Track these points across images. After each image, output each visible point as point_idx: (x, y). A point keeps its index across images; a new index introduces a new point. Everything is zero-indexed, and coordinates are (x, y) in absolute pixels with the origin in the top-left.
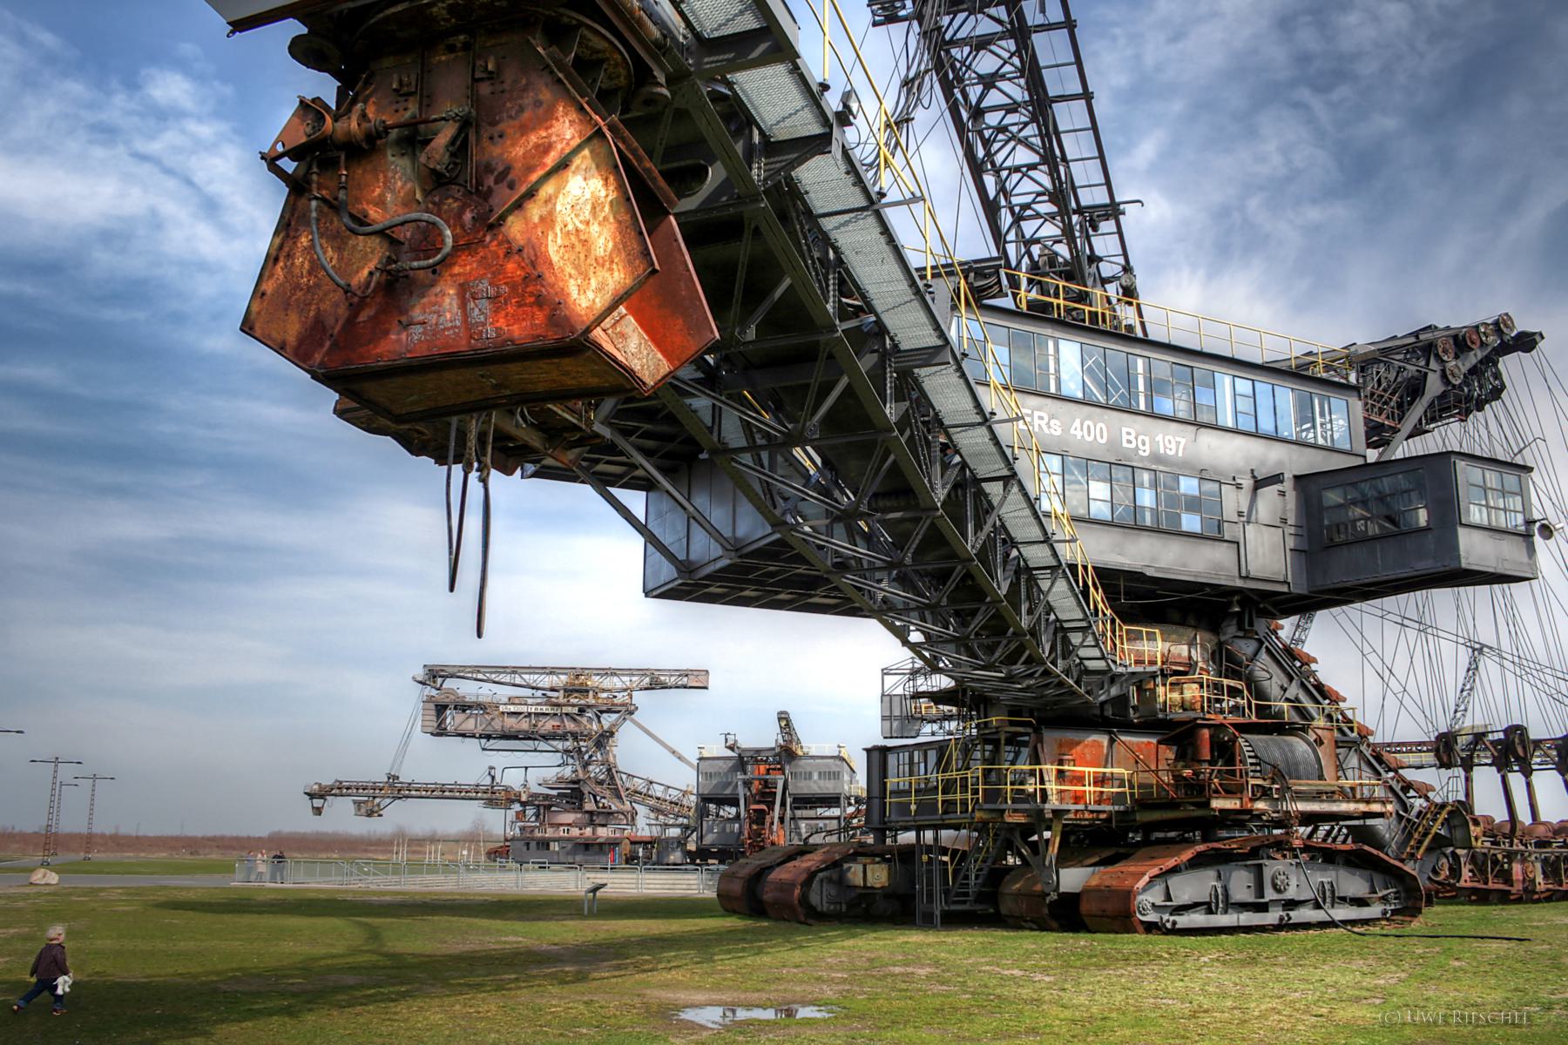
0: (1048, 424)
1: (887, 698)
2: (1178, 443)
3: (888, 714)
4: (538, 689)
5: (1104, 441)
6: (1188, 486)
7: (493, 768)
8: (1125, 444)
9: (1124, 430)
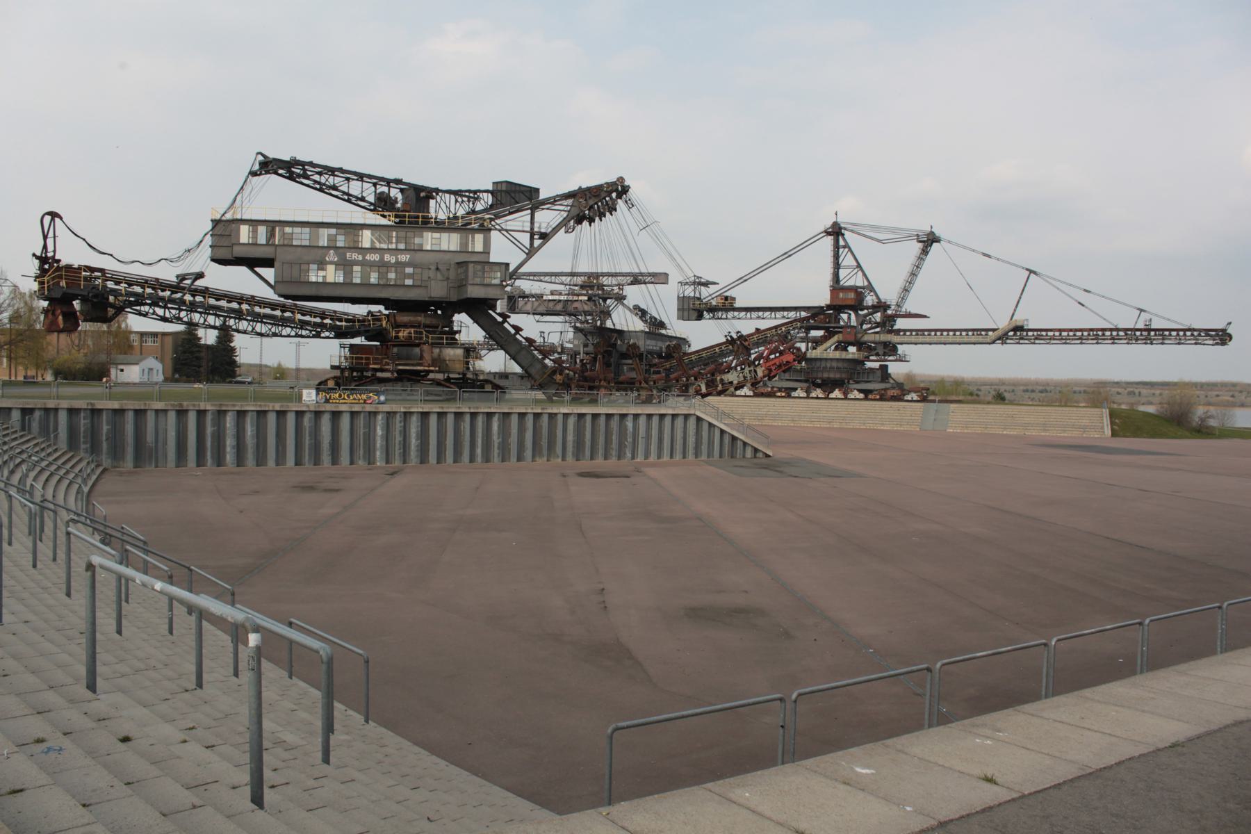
2: (406, 257)
4: (566, 285)
6: (409, 270)
7: (543, 333)
9: (386, 255)
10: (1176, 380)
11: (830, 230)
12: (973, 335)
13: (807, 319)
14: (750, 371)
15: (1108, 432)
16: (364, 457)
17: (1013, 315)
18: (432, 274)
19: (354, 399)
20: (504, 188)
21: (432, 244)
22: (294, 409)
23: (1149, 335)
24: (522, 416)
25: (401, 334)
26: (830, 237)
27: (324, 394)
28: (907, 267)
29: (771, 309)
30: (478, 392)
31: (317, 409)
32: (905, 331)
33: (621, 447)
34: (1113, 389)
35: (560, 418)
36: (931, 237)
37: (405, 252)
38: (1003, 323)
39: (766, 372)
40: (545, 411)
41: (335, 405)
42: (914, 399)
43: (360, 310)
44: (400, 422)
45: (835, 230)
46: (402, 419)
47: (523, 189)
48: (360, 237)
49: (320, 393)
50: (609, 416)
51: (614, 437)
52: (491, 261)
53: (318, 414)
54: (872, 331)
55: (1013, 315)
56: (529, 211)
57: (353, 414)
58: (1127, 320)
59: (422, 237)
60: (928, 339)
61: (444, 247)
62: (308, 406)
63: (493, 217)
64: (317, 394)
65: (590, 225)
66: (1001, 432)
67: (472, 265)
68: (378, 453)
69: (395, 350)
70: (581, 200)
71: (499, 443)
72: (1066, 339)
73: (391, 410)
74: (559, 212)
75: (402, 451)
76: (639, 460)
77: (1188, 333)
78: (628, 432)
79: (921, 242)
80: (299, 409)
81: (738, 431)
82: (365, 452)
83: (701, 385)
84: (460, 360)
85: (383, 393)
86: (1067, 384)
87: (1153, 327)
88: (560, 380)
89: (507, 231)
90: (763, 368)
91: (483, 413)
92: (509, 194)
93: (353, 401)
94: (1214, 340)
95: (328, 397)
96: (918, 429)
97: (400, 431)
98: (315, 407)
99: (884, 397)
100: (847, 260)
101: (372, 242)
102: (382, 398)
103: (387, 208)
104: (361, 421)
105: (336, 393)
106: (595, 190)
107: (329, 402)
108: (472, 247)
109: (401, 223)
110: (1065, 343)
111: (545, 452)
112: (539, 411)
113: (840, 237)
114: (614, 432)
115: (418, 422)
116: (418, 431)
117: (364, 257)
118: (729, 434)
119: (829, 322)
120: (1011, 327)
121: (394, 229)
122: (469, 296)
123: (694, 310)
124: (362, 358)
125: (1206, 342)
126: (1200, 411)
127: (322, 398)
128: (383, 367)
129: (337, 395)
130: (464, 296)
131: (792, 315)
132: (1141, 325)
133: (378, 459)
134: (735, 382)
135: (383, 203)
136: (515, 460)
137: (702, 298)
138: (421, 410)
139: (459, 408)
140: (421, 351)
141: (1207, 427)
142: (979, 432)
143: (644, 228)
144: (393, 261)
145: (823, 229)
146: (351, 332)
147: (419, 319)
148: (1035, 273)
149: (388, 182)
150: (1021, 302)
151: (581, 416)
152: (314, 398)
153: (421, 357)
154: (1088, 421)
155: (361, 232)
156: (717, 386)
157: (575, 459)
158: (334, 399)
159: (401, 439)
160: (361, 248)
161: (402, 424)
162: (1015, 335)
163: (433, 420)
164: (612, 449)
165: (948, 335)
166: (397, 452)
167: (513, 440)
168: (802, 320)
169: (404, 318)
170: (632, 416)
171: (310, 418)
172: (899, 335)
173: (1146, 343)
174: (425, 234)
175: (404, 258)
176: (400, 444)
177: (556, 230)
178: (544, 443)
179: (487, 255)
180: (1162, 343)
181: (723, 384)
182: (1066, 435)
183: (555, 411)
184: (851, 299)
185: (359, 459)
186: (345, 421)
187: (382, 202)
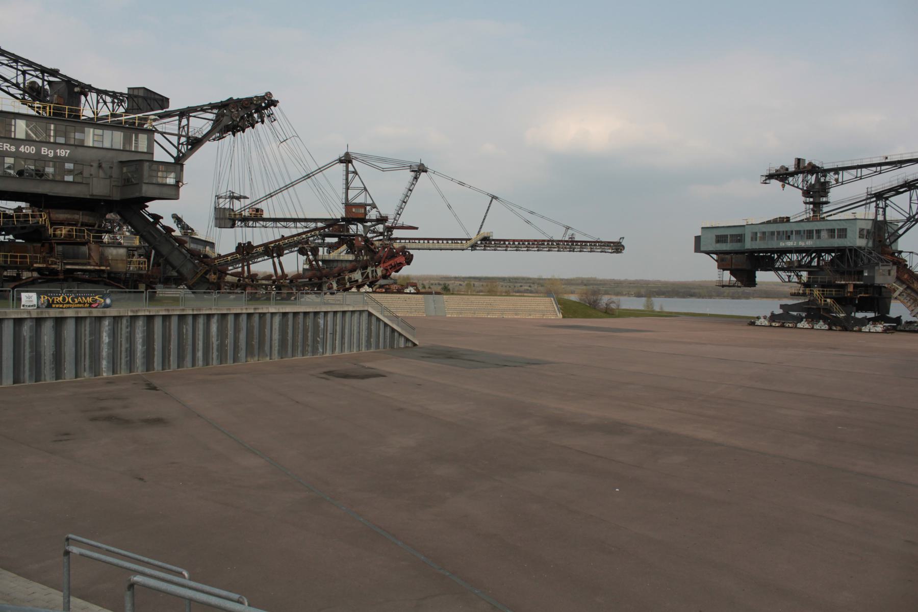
0: (10, 148)
1: (217, 210)
2: (66, 152)
3: (218, 217)
5: (34, 152)
6: (69, 166)
8: (43, 153)
9: (43, 148)
10: (549, 277)
11: (343, 158)
12: (410, 242)
13: (323, 228)
14: (373, 271)
15: (560, 316)
16: (91, 368)
17: (481, 228)
18: (93, 171)
19: (79, 303)
20: (141, 93)
21: (94, 141)
22: (13, 317)
23: (571, 245)
24: (237, 316)
25: (58, 232)
26: (342, 164)
27: (46, 297)
28: (403, 190)
29: (295, 220)
30: (130, 292)
31: (40, 316)
32: (401, 239)
33: (315, 341)
34: (456, 282)
35: (268, 316)
36: (421, 168)
37: (65, 146)
38: (473, 235)
39: (384, 272)
40: (257, 311)
41: (61, 310)
42: (412, 292)
43: (13, 205)
44: (127, 328)
45: (348, 159)
46: (129, 324)
47: (156, 97)
48: (13, 127)
49: (42, 296)
50: (306, 314)
51: (309, 334)
52: (155, 159)
53: (39, 321)
54: (377, 238)
55: (481, 228)
56: (177, 118)
57: (78, 320)
58: (558, 235)
59: (83, 132)
60: (431, 245)
61: (107, 145)
62: (29, 312)
63: (157, 117)
64: (39, 298)
65: (234, 136)
66: (486, 316)
67: (148, 163)
68: (104, 363)
69: (59, 248)
70: (233, 110)
71: (218, 345)
72: (518, 247)
73: (119, 315)
74: (207, 121)
75: (129, 358)
76: (327, 355)
77: (597, 244)
78: (320, 329)
79: (412, 171)
80: (19, 316)
81: (398, 325)
82: (91, 362)
83: (333, 283)
84: (122, 260)
85: (108, 295)
86: (604, 280)
87: (576, 239)
88: (214, 279)
89: (162, 133)
90: (382, 269)
91: (203, 314)
92: (146, 101)
93: (78, 305)
94: (612, 249)
95: (51, 300)
96: (425, 315)
97: (127, 337)
98: (38, 313)
99: (389, 290)
100: (356, 183)
101: (27, 133)
102: (108, 301)
103: (41, 99)
104: (87, 327)
105: (59, 297)
106: (246, 102)
107: (52, 307)
108: (135, 146)
109: (57, 115)
110: (517, 250)
111: (256, 351)
112: (252, 311)
113: (350, 165)
114: (310, 329)
115: (144, 327)
116: (144, 336)
117: (17, 149)
118: (390, 326)
119: (342, 232)
120: (480, 237)
121: (51, 121)
122: (144, 195)
123: (230, 219)
124: (16, 257)
125: (606, 250)
126: (605, 299)
127: (44, 302)
128: (49, 266)
129: (61, 299)
130: (141, 195)
131: (312, 225)
132: (567, 239)
133: (104, 369)
134: (360, 280)
135: (33, 93)
136: (232, 361)
137: (235, 210)
138: (147, 313)
139: (183, 310)
140: (89, 249)
141: (612, 310)
142: (470, 316)
143: (284, 141)
144: (51, 155)
145: (337, 157)
146: (7, 228)
147: (76, 217)
148: (496, 198)
149: (44, 70)
150: (487, 217)
151: (285, 314)
152: (35, 302)
153: (90, 257)
154: (544, 307)
155: (13, 121)
156: (345, 284)
157: (280, 358)
158: (58, 303)
159: (128, 345)
160: (15, 139)
161: (129, 330)
162: (481, 243)
163: (158, 324)
164: (308, 346)
165: (443, 243)
166: (123, 361)
167: (230, 341)
168: (316, 229)
169: (61, 215)
170: (323, 314)
171: (31, 327)
172: (396, 242)
173: (570, 251)
174: (86, 129)
175: (63, 153)
176: (126, 351)
177: (207, 137)
178: (255, 342)
179: (151, 155)
180: (580, 251)
181: (350, 283)
182: (532, 317)
183: (265, 311)
184: (362, 213)
185: (85, 371)
186: (69, 330)
187: (34, 92)
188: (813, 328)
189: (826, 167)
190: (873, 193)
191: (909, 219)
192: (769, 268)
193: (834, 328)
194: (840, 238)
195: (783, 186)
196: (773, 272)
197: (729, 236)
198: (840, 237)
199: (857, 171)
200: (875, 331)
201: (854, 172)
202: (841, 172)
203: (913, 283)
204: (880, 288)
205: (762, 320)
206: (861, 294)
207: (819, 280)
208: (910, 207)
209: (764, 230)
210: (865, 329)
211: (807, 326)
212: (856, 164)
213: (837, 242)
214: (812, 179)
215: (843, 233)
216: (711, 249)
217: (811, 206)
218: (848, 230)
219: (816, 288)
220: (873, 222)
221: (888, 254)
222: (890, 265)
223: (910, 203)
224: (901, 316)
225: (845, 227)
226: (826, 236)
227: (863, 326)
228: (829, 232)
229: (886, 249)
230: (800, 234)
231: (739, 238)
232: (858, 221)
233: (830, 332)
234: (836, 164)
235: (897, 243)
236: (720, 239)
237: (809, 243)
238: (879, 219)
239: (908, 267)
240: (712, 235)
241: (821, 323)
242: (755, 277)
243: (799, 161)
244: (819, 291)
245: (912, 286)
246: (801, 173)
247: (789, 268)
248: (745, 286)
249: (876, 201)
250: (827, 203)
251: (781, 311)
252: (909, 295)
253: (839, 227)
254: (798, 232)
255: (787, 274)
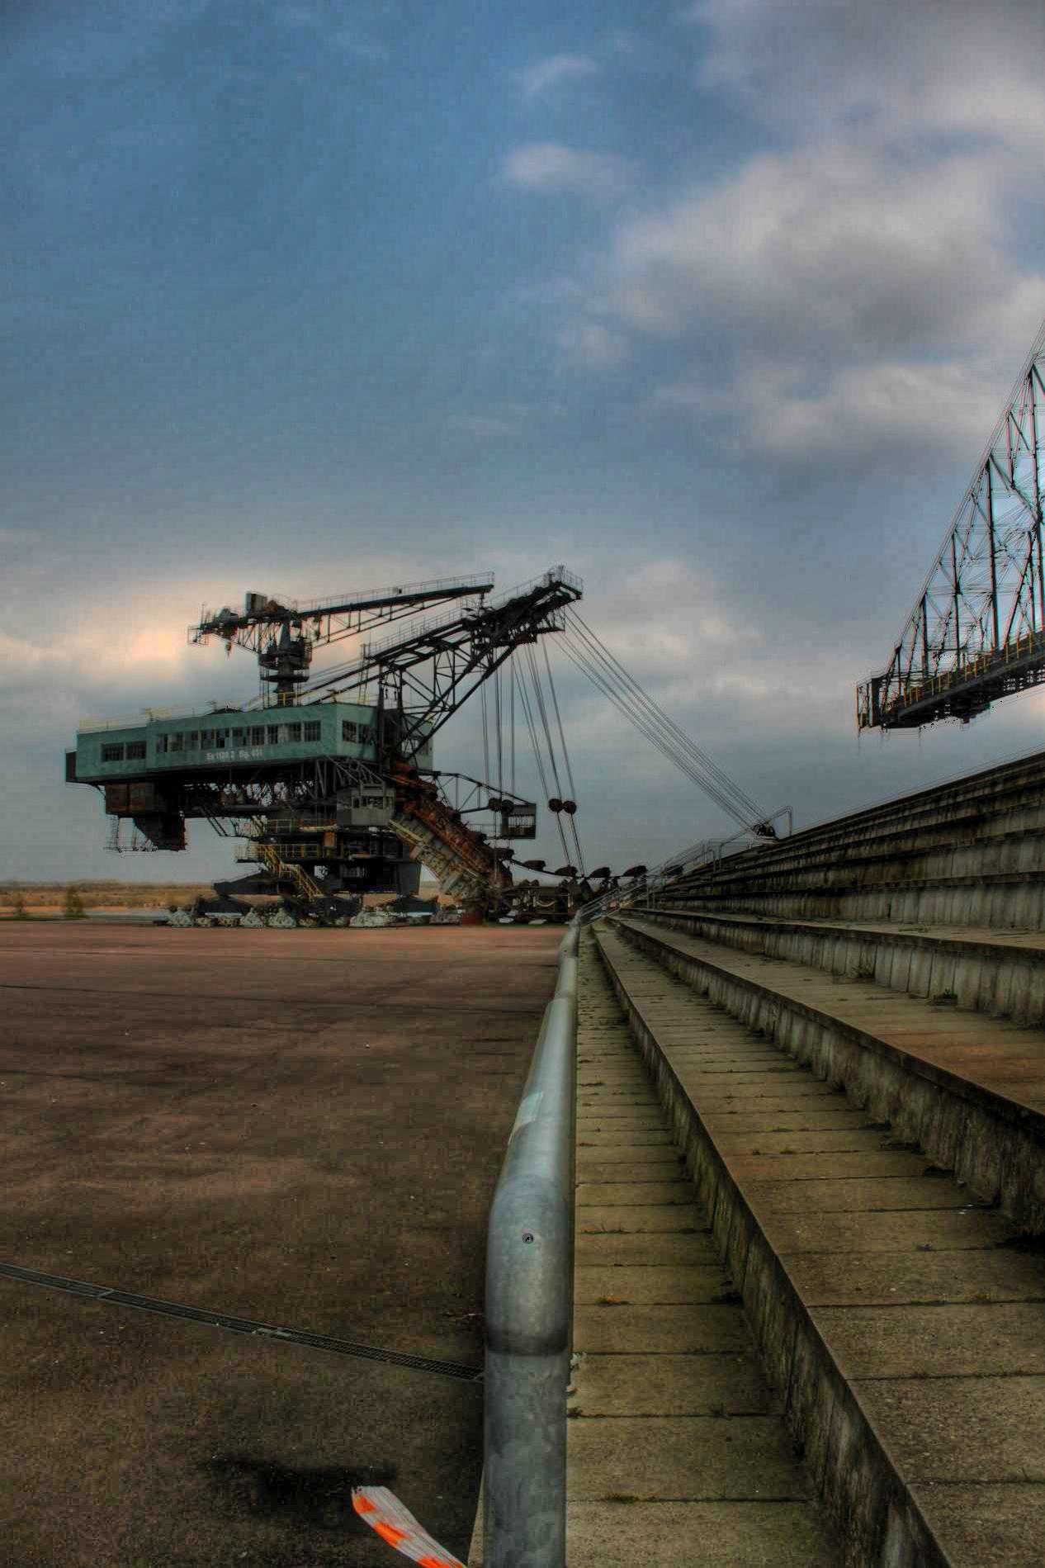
188: (267, 925)
189: (301, 609)
190: (373, 655)
191: (434, 704)
192: (196, 808)
193: (303, 922)
194: (309, 740)
195: (229, 648)
196: (205, 819)
197: (125, 746)
198: (309, 738)
199: (350, 617)
200: (371, 925)
201: (344, 617)
202: (325, 619)
203: (444, 828)
204: (386, 840)
205: (179, 913)
206: (356, 851)
207: (290, 827)
208: (435, 679)
209: (179, 729)
210: (355, 921)
211: (257, 921)
212: (348, 603)
213: (304, 750)
214: (277, 632)
215: (313, 731)
216: (94, 772)
217: (274, 686)
218: (322, 724)
219: (272, 842)
220: (374, 712)
221: (402, 773)
222: (380, 788)
223: (436, 673)
224: (437, 898)
225: (317, 719)
226: (287, 736)
227: (350, 915)
228: (290, 729)
229: (402, 765)
230: (241, 735)
231: (138, 750)
232: (338, 705)
233: (300, 931)
234: (318, 603)
235: (432, 756)
236: (111, 753)
237: (254, 754)
238: (386, 707)
239: (439, 800)
240: (97, 746)
241: (281, 913)
242: (184, 830)
243: (253, 598)
244: (277, 849)
245: (443, 835)
246: (260, 619)
247: (249, 809)
248: (161, 847)
249: (381, 676)
250: (305, 679)
251: (214, 895)
252: (436, 852)
253: (306, 719)
254: (238, 732)
255: (233, 819)
